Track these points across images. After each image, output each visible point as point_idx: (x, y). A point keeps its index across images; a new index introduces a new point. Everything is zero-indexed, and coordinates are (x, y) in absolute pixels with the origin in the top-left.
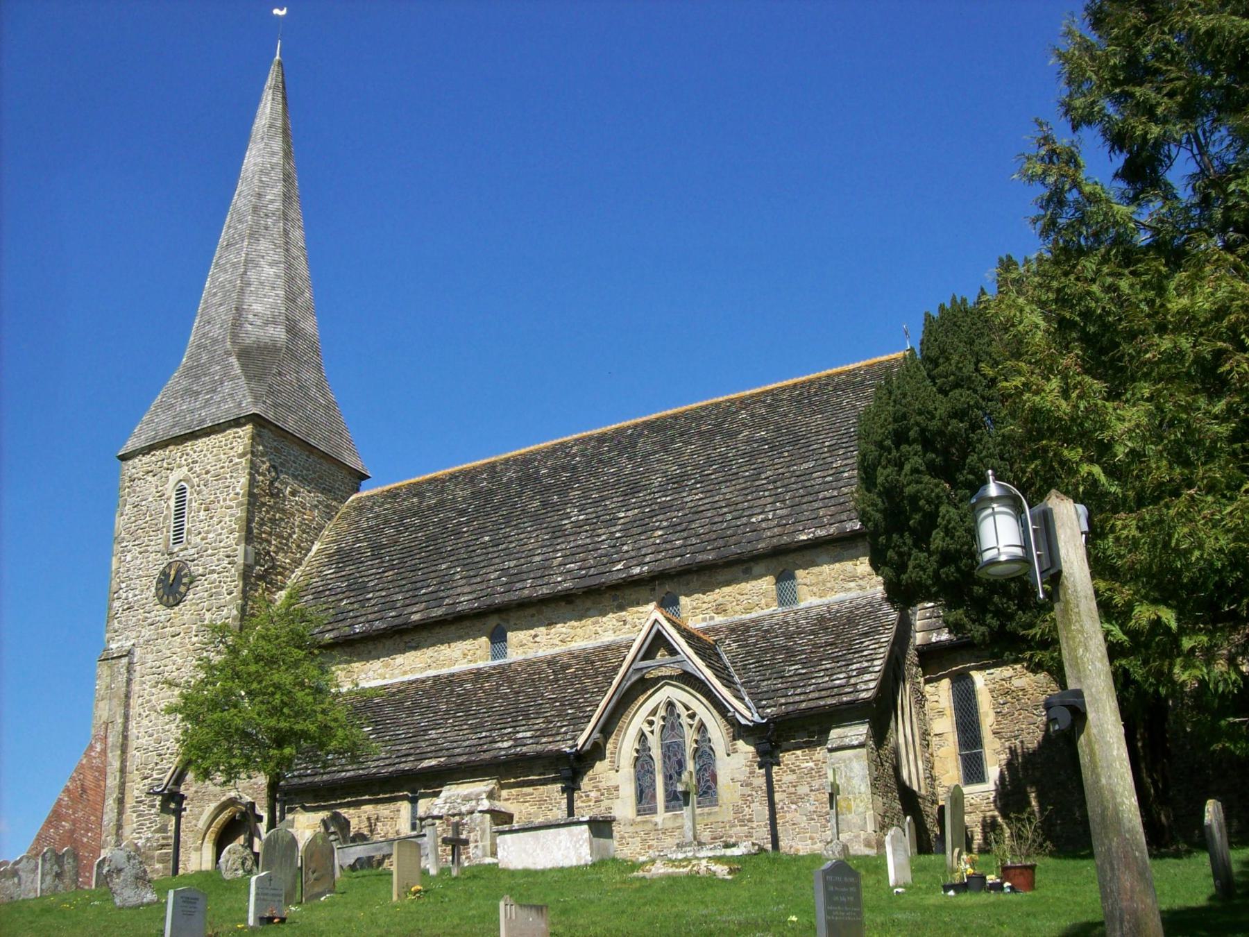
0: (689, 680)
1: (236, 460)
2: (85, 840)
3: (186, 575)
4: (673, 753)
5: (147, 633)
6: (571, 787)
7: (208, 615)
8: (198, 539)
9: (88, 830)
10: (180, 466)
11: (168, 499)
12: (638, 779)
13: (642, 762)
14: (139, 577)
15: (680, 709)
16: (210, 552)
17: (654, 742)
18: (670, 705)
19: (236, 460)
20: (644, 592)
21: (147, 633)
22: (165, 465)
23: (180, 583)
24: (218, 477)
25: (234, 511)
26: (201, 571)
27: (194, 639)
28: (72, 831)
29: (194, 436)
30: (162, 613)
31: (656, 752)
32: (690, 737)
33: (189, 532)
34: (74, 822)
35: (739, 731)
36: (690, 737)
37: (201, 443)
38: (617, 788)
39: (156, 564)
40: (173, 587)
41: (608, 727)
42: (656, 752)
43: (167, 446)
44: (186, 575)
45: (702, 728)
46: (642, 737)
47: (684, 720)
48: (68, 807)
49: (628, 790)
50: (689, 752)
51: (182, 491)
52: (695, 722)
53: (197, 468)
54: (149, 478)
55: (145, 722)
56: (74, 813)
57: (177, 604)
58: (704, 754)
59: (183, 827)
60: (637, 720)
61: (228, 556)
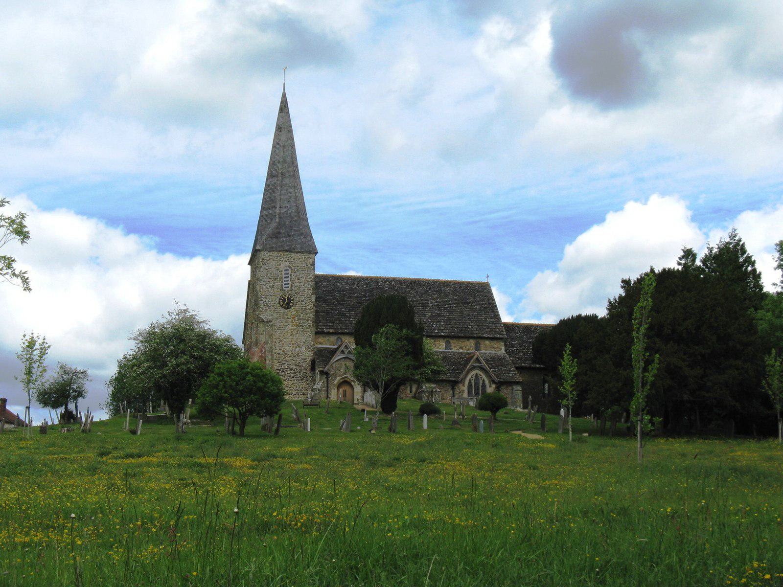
0: (482, 369)
1: (309, 266)
4: (477, 384)
5: (276, 315)
6: (453, 389)
7: (302, 315)
11: (282, 271)
12: (468, 389)
13: (470, 386)
14: (271, 295)
15: (479, 375)
18: (477, 374)
19: (309, 266)
21: (276, 315)
23: (290, 302)
25: (310, 283)
26: (297, 299)
30: (283, 310)
31: (473, 384)
36: (481, 382)
38: (464, 390)
40: (287, 303)
42: (473, 384)
44: (292, 300)
45: (484, 381)
46: (470, 380)
47: (479, 378)
49: (466, 391)
50: (481, 384)
52: (482, 379)
54: (272, 261)
58: (484, 386)
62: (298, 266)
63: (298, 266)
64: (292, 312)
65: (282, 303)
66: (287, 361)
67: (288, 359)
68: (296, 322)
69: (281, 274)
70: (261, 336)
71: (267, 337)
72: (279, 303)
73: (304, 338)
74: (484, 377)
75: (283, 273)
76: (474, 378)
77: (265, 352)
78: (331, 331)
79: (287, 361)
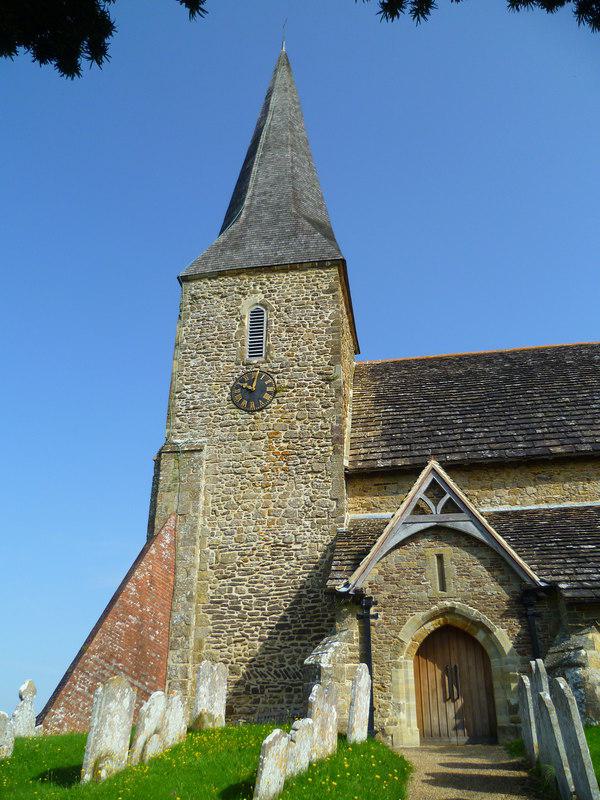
2: (153, 638)
3: (270, 385)
7: (298, 424)
9: (154, 628)
10: (254, 292)
11: (243, 317)
16: (296, 367)
22: (235, 289)
23: (264, 391)
24: (302, 306)
26: (287, 383)
27: (282, 444)
28: (139, 627)
29: (269, 269)
30: (241, 416)
33: (268, 348)
34: (142, 616)
37: (277, 278)
39: (228, 368)
43: (239, 274)
44: (270, 385)
48: (134, 599)
51: (257, 315)
53: (275, 296)
55: (221, 520)
56: (142, 606)
57: (261, 410)
59: (374, 636)
61: (320, 374)
62: (288, 301)
63: (288, 301)
64: (271, 416)
65: (239, 397)
66: (247, 572)
67: (252, 564)
68: (282, 444)
70: (168, 496)
71: (186, 495)
73: (304, 494)
75: (247, 321)
78: (400, 463)
79: (247, 572)
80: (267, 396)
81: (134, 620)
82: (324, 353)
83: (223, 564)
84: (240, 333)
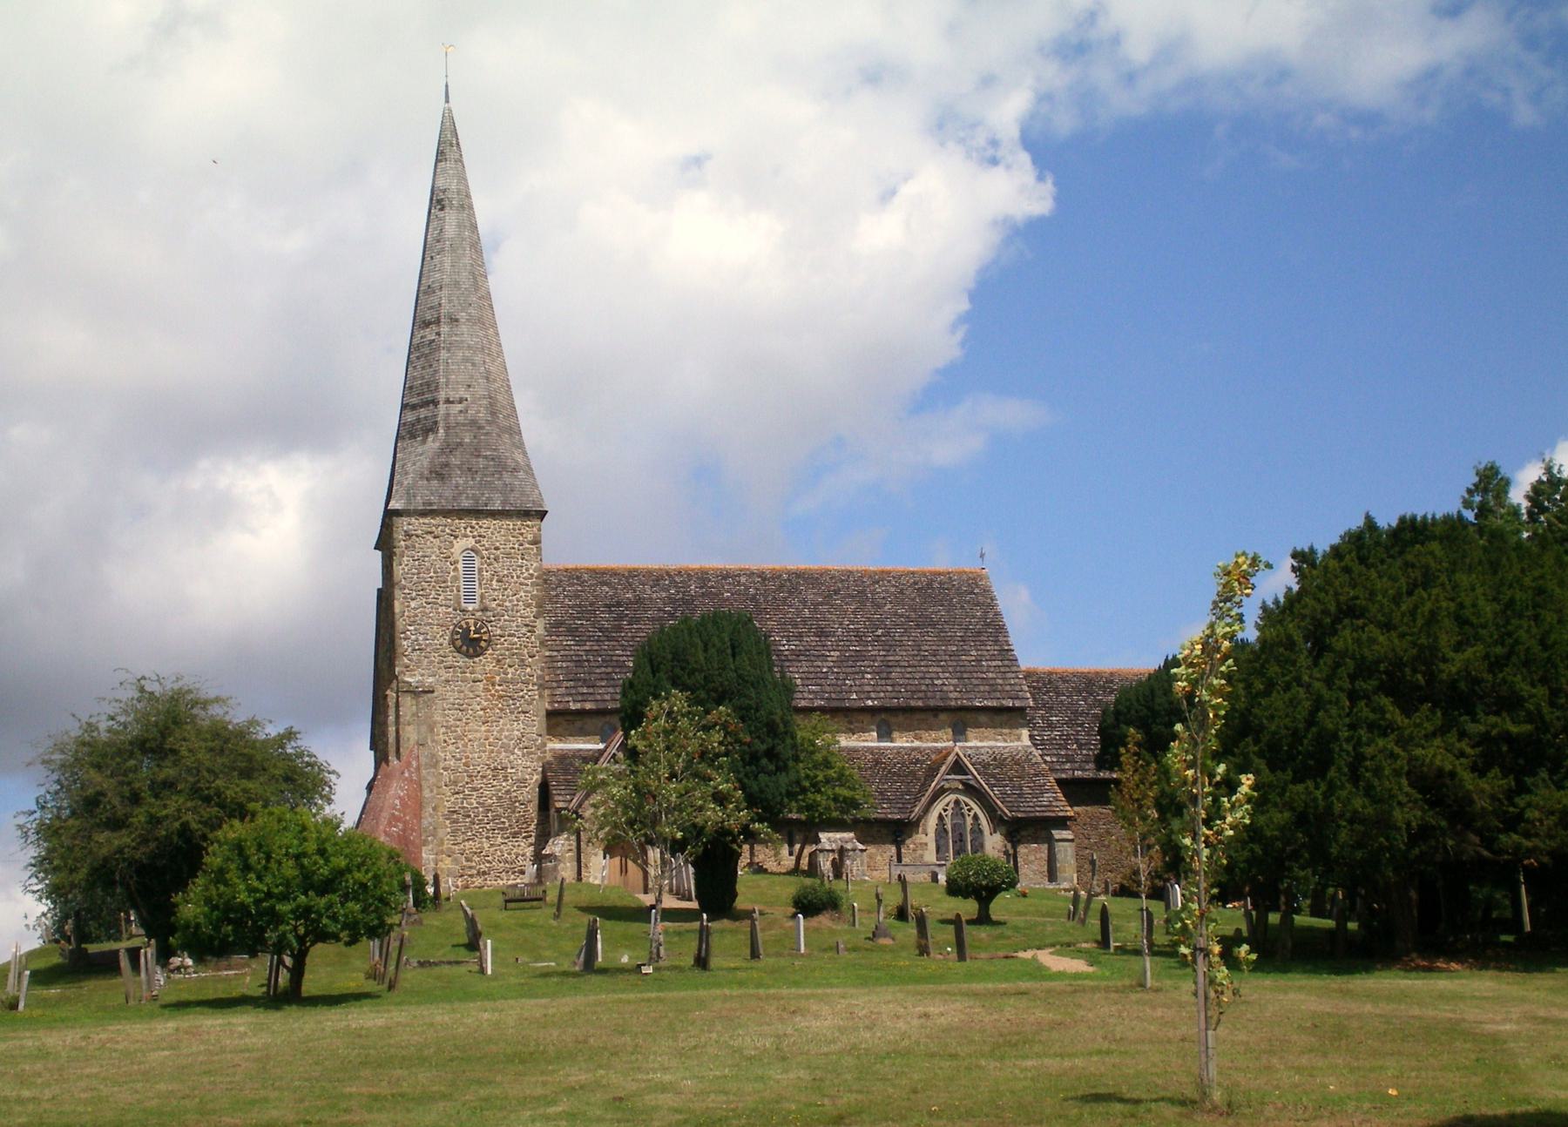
0: (971, 790)
5: (445, 675)
8: (494, 605)
11: (456, 562)
13: (941, 832)
17: (948, 821)
18: (957, 802)
20: (866, 718)
21: (445, 675)
24: (509, 556)
30: (462, 661)
32: (969, 820)
34: (405, 823)
35: (997, 820)
36: (969, 820)
37: (485, 522)
41: (926, 810)
45: (976, 817)
46: (941, 817)
49: (932, 846)
50: (969, 827)
54: (429, 537)
55: (451, 748)
58: (977, 831)
60: (938, 808)
62: (497, 549)
63: (497, 549)
64: (486, 663)
65: (459, 643)
66: (474, 789)
67: (477, 783)
69: (456, 569)
70: (409, 728)
71: (424, 729)
72: (452, 642)
73: (517, 729)
74: (976, 809)
75: (460, 566)
76: (950, 812)
77: (418, 768)
78: (588, 706)
79: (474, 789)
80: (483, 644)
81: (401, 826)
82: (529, 606)
83: (455, 783)
84: (456, 578)
